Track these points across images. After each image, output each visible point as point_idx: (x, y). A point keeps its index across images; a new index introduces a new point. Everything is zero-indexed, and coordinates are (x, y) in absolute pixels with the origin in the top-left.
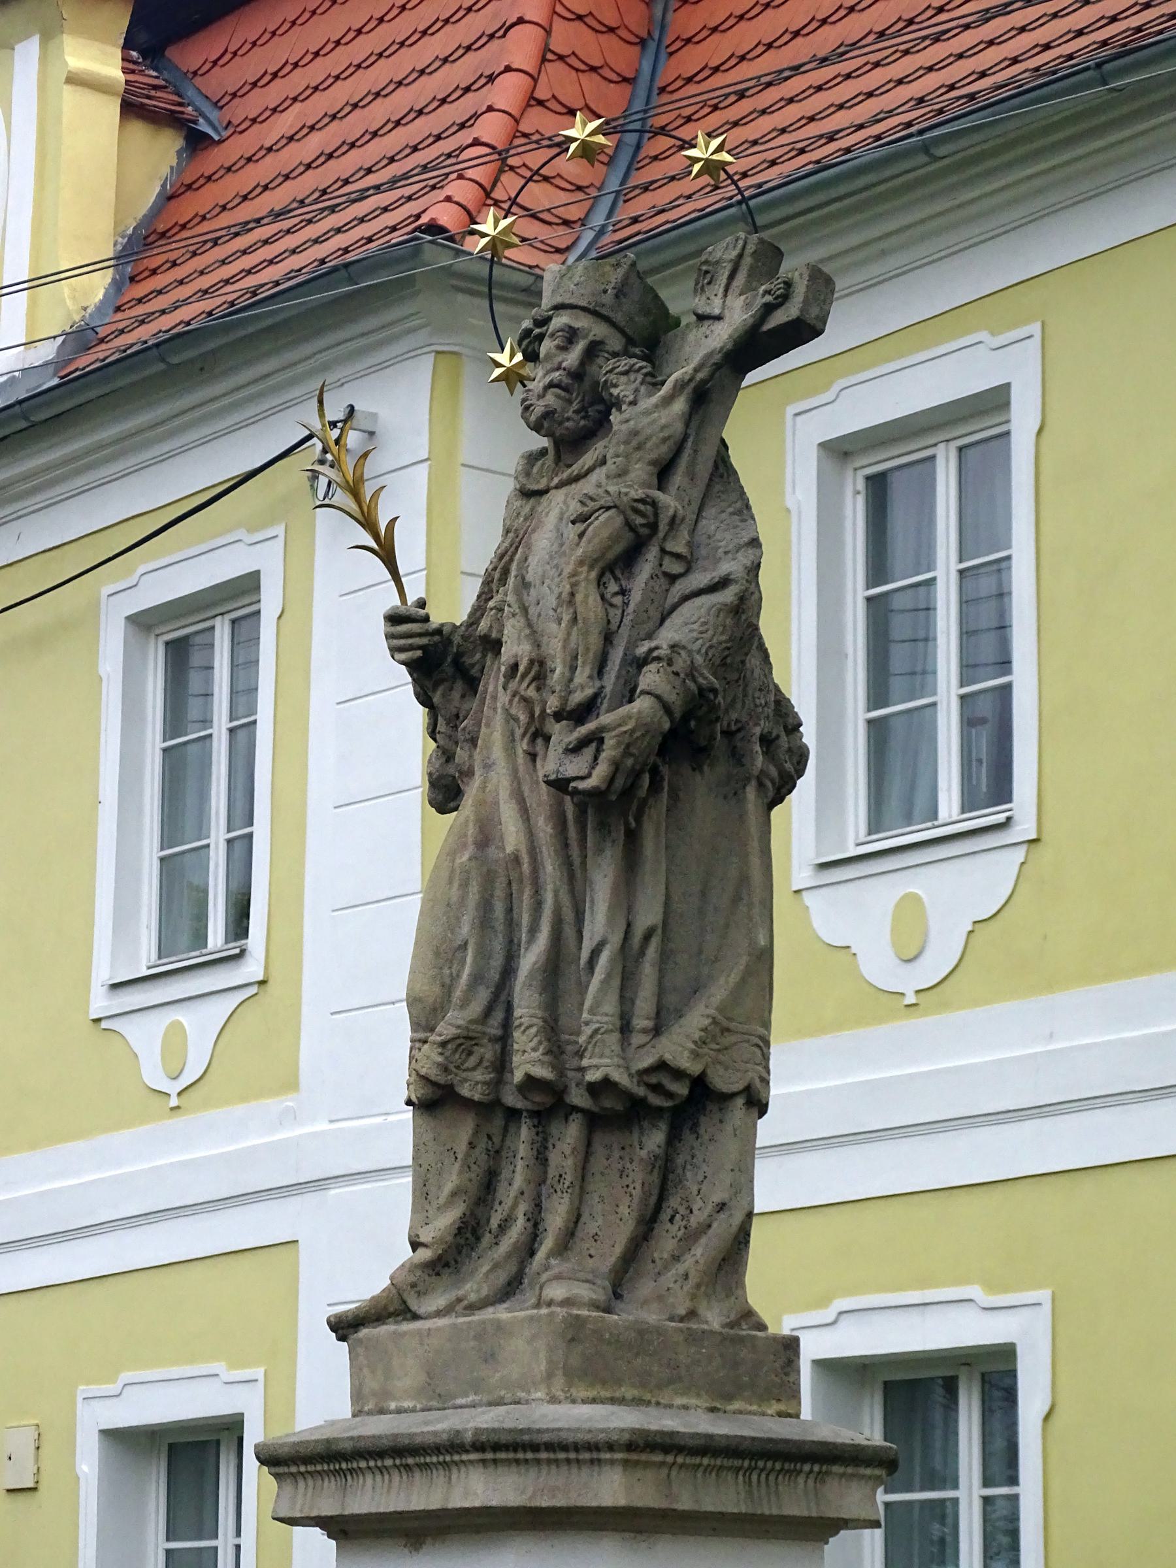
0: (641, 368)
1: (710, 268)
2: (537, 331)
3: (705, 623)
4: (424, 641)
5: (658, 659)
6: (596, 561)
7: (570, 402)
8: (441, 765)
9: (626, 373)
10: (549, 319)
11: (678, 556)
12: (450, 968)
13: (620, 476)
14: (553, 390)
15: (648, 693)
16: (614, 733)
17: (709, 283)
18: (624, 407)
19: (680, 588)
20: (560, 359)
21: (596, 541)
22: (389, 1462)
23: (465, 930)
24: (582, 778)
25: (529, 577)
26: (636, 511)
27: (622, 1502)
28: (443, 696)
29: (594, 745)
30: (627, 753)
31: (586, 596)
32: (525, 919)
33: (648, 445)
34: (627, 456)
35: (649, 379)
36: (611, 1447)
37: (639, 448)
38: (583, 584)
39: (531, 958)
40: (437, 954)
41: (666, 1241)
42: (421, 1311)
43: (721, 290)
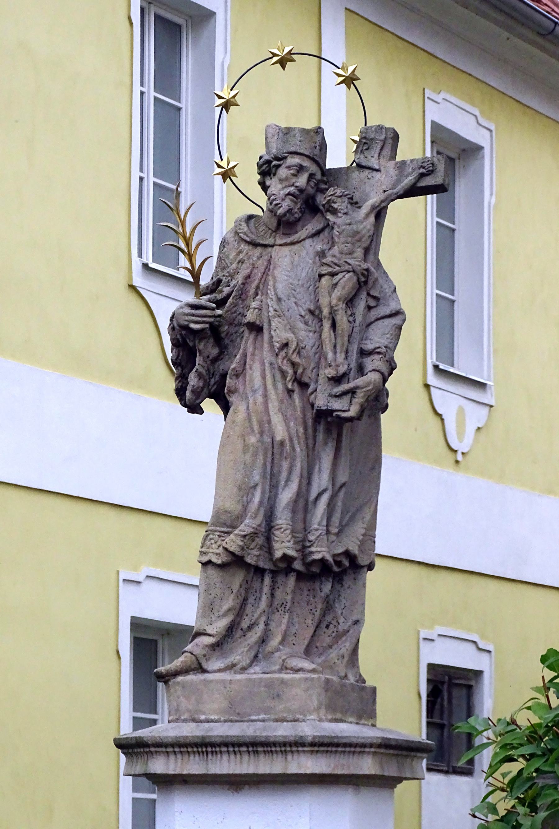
0: (347, 195)
1: (368, 141)
2: (275, 163)
3: (392, 335)
4: (212, 320)
5: (379, 353)
6: (346, 298)
7: (296, 203)
8: (198, 381)
9: (340, 197)
10: (286, 158)
11: (374, 298)
12: (247, 497)
13: (350, 254)
14: (291, 197)
15: (378, 371)
16: (363, 390)
17: (367, 149)
18: (340, 215)
19: (374, 314)
20: (294, 180)
21: (346, 289)
22: (244, 749)
23: (257, 477)
24: (344, 411)
25: (281, 295)
26: (363, 274)
27: (373, 772)
28: (204, 345)
29: (350, 394)
30: (367, 400)
31: (342, 317)
32: (284, 475)
33: (363, 240)
34: (353, 244)
35: (350, 200)
36: (371, 745)
37: (359, 241)
38: (341, 311)
39: (286, 496)
40: (240, 489)
41: (325, 639)
42: (209, 669)
43: (376, 156)
